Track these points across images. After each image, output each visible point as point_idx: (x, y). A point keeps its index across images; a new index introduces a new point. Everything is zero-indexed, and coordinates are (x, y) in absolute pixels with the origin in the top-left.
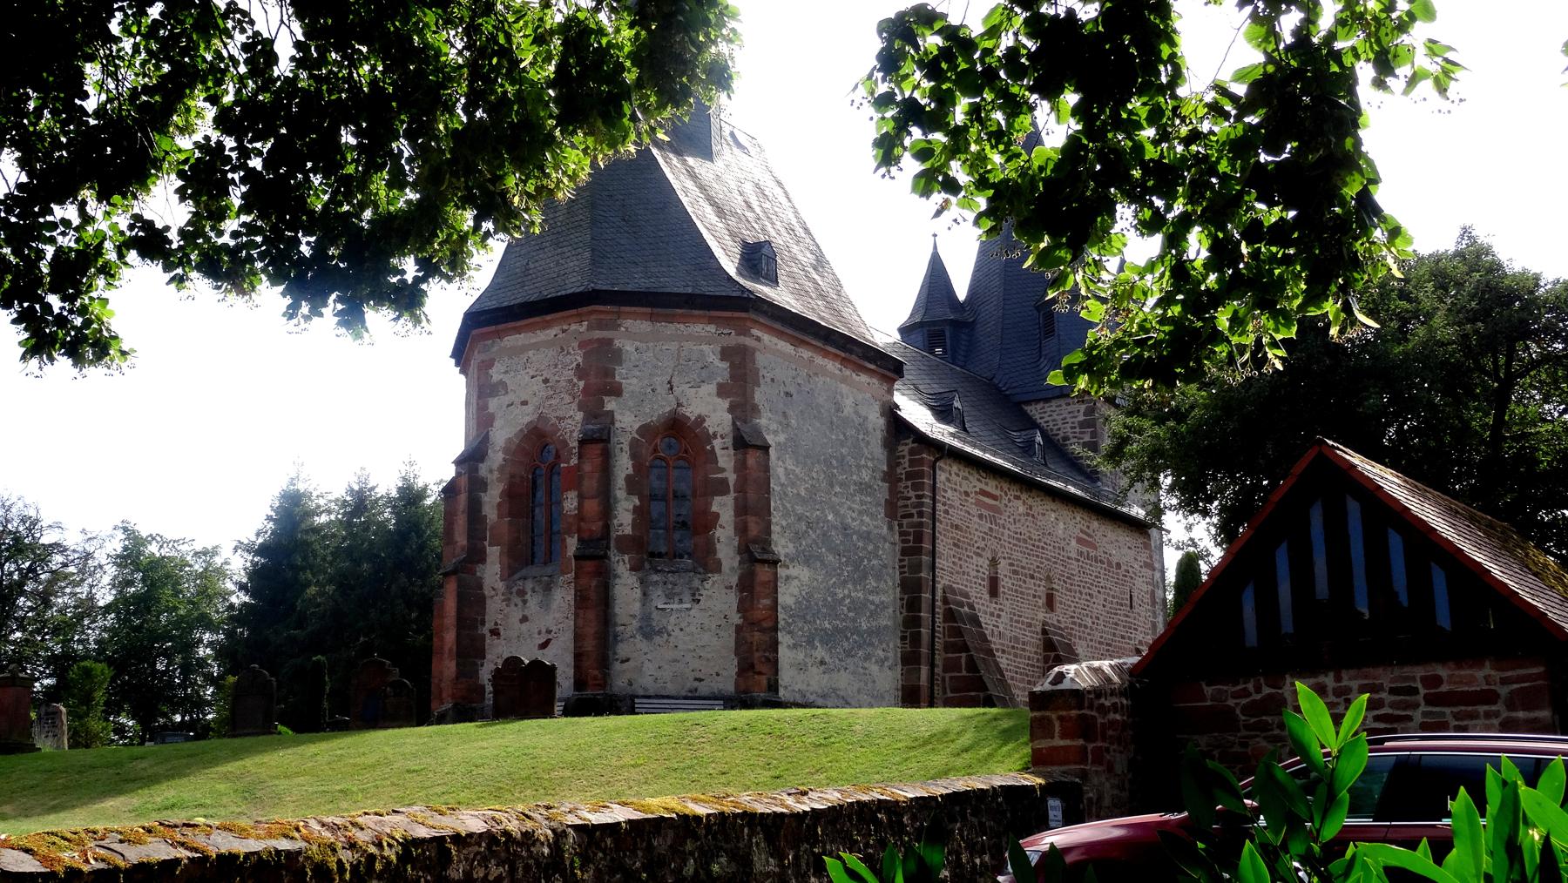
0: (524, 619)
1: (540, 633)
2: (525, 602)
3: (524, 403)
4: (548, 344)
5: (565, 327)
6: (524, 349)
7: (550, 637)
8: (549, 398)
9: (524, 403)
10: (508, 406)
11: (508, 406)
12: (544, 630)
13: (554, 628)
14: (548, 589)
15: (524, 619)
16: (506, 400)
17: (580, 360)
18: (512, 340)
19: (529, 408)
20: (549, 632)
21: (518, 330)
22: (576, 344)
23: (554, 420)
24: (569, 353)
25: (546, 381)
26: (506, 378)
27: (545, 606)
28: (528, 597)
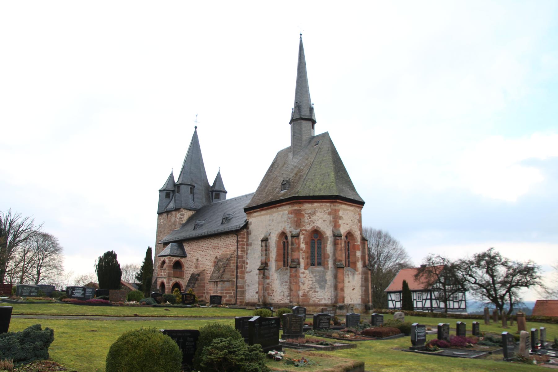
0: (349, 282)
1: (352, 286)
2: (349, 277)
3: (347, 224)
4: (352, 211)
6: (346, 210)
7: (355, 287)
8: (353, 225)
9: (347, 224)
13: (355, 285)
14: (354, 275)
15: (349, 282)
16: (344, 222)
18: (343, 206)
19: (348, 226)
21: (346, 204)
22: (357, 214)
23: (354, 231)
25: (352, 220)
26: (343, 216)
27: (353, 279)
28: (350, 276)
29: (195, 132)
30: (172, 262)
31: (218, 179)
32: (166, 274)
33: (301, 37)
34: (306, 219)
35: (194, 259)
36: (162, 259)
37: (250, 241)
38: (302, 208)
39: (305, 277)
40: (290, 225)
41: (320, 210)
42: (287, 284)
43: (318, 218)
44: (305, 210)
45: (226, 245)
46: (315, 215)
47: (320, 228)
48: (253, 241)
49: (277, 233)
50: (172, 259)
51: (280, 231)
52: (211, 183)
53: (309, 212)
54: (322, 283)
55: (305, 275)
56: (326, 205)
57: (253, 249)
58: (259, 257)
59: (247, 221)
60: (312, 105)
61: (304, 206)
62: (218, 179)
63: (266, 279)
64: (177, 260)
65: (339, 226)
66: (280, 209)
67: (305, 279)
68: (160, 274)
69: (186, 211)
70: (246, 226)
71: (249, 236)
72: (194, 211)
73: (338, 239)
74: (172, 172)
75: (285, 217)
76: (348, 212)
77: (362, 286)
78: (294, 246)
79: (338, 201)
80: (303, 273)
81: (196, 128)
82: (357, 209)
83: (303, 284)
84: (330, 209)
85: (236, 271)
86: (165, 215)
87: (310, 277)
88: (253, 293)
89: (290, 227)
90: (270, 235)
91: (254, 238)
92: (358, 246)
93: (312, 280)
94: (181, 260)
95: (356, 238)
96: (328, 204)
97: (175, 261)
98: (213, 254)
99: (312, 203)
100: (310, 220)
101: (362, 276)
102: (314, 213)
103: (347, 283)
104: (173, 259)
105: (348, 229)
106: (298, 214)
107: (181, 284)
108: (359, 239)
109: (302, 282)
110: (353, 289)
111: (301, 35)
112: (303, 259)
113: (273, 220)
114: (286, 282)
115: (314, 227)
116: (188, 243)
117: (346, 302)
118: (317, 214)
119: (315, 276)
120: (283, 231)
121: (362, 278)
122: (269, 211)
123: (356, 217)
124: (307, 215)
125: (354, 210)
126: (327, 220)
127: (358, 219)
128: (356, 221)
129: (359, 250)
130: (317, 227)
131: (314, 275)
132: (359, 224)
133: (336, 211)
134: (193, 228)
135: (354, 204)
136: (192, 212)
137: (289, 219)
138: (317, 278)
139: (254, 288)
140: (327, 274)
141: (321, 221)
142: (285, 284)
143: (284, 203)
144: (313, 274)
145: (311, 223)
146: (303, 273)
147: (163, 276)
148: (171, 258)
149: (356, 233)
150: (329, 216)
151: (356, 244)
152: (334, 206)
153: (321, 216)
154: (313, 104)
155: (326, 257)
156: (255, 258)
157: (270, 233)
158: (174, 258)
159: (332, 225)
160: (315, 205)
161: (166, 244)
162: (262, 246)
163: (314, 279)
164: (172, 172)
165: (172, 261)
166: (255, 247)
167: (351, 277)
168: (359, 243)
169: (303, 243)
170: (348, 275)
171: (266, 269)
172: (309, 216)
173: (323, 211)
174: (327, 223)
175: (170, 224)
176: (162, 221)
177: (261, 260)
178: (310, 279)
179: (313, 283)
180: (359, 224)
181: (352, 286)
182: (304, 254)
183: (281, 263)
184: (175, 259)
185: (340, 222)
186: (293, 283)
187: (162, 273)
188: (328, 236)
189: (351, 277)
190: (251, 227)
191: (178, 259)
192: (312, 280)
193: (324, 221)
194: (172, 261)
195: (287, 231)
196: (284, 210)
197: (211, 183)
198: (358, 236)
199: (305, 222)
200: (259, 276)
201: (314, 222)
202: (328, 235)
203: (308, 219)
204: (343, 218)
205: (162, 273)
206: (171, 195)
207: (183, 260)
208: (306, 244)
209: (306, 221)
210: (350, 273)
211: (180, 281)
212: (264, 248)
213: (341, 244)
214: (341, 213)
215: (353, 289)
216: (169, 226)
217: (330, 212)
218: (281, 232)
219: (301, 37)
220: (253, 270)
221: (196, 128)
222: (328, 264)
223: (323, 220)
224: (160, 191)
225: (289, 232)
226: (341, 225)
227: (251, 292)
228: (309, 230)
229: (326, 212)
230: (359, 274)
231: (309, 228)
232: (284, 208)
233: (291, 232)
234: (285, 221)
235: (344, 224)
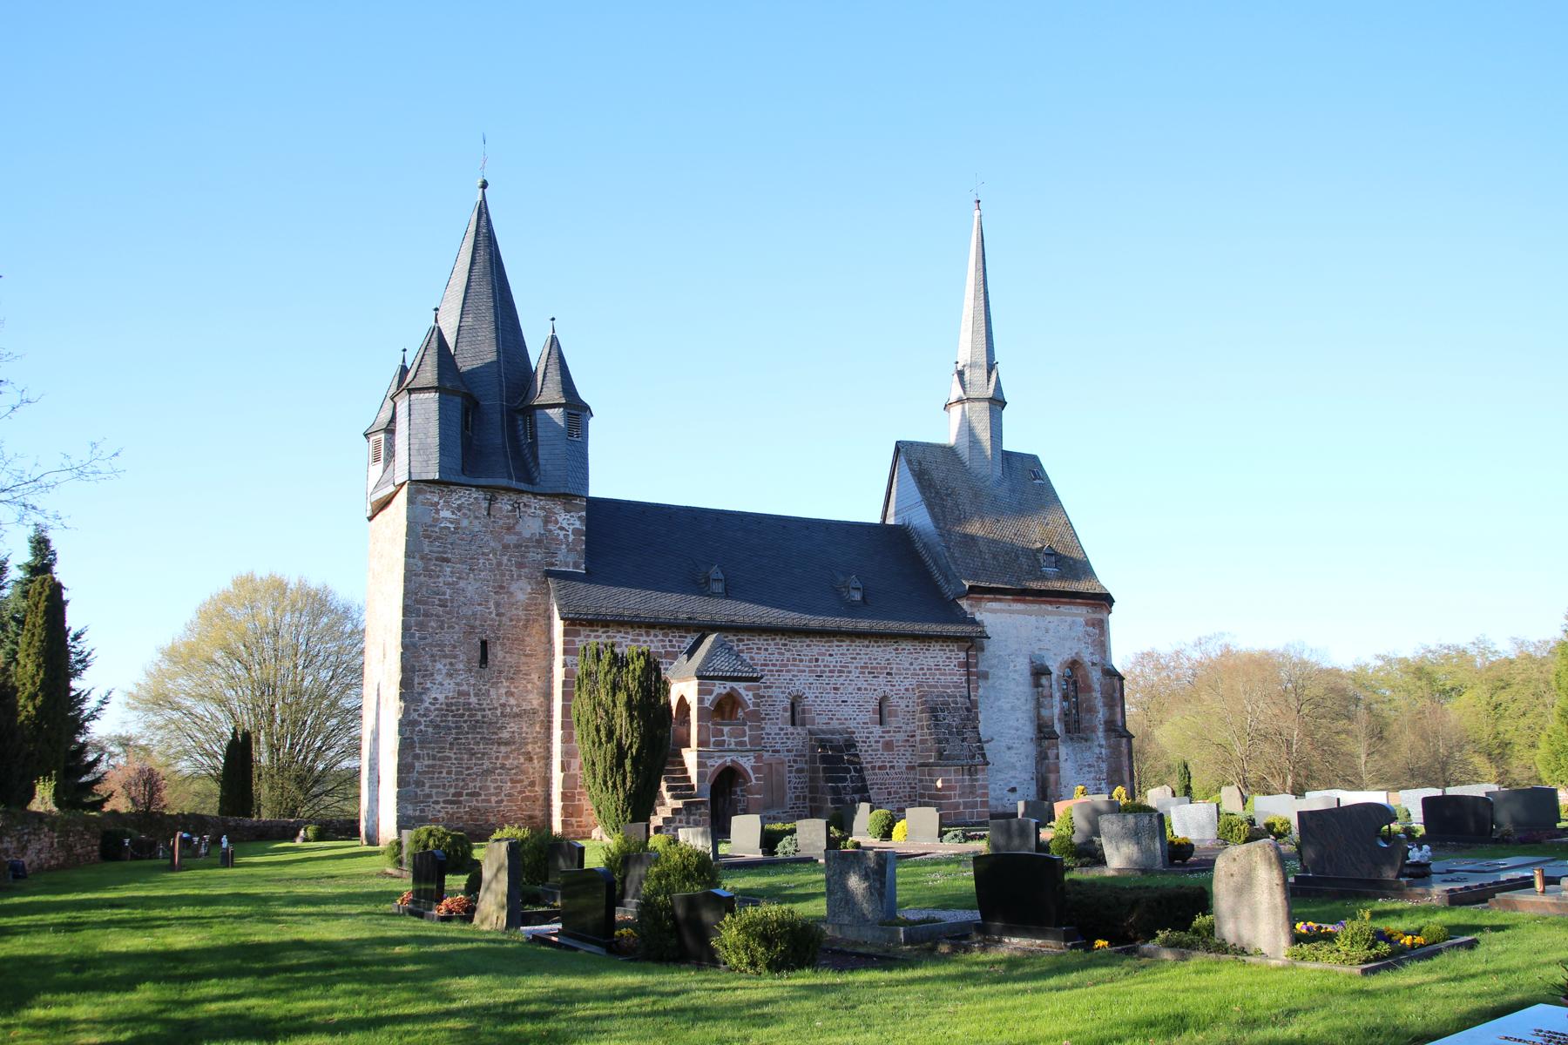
37: (982, 667)
45: (923, 669)
48: (991, 668)
49: (1060, 659)
51: (1067, 656)
57: (993, 687)
66: (1063, 609)
74: (436, 321)
88: (998, 792)
89: (1092, 654)
91: (995, 661)
114: (1090, 766)
122: (1035, 607)
137: (1089, 635)
139: (1002, 780)
142: (1087, 769)
143: (1078, 601)
147: (732, 747)
156: (1000, 710)
164: (436, 321)
166: (1001, 684)
184: (720, 689)
196: (1076, 615)
220: (995, 737)
221: (484, 185)
227: (995, 790)
232: (1074, 609)
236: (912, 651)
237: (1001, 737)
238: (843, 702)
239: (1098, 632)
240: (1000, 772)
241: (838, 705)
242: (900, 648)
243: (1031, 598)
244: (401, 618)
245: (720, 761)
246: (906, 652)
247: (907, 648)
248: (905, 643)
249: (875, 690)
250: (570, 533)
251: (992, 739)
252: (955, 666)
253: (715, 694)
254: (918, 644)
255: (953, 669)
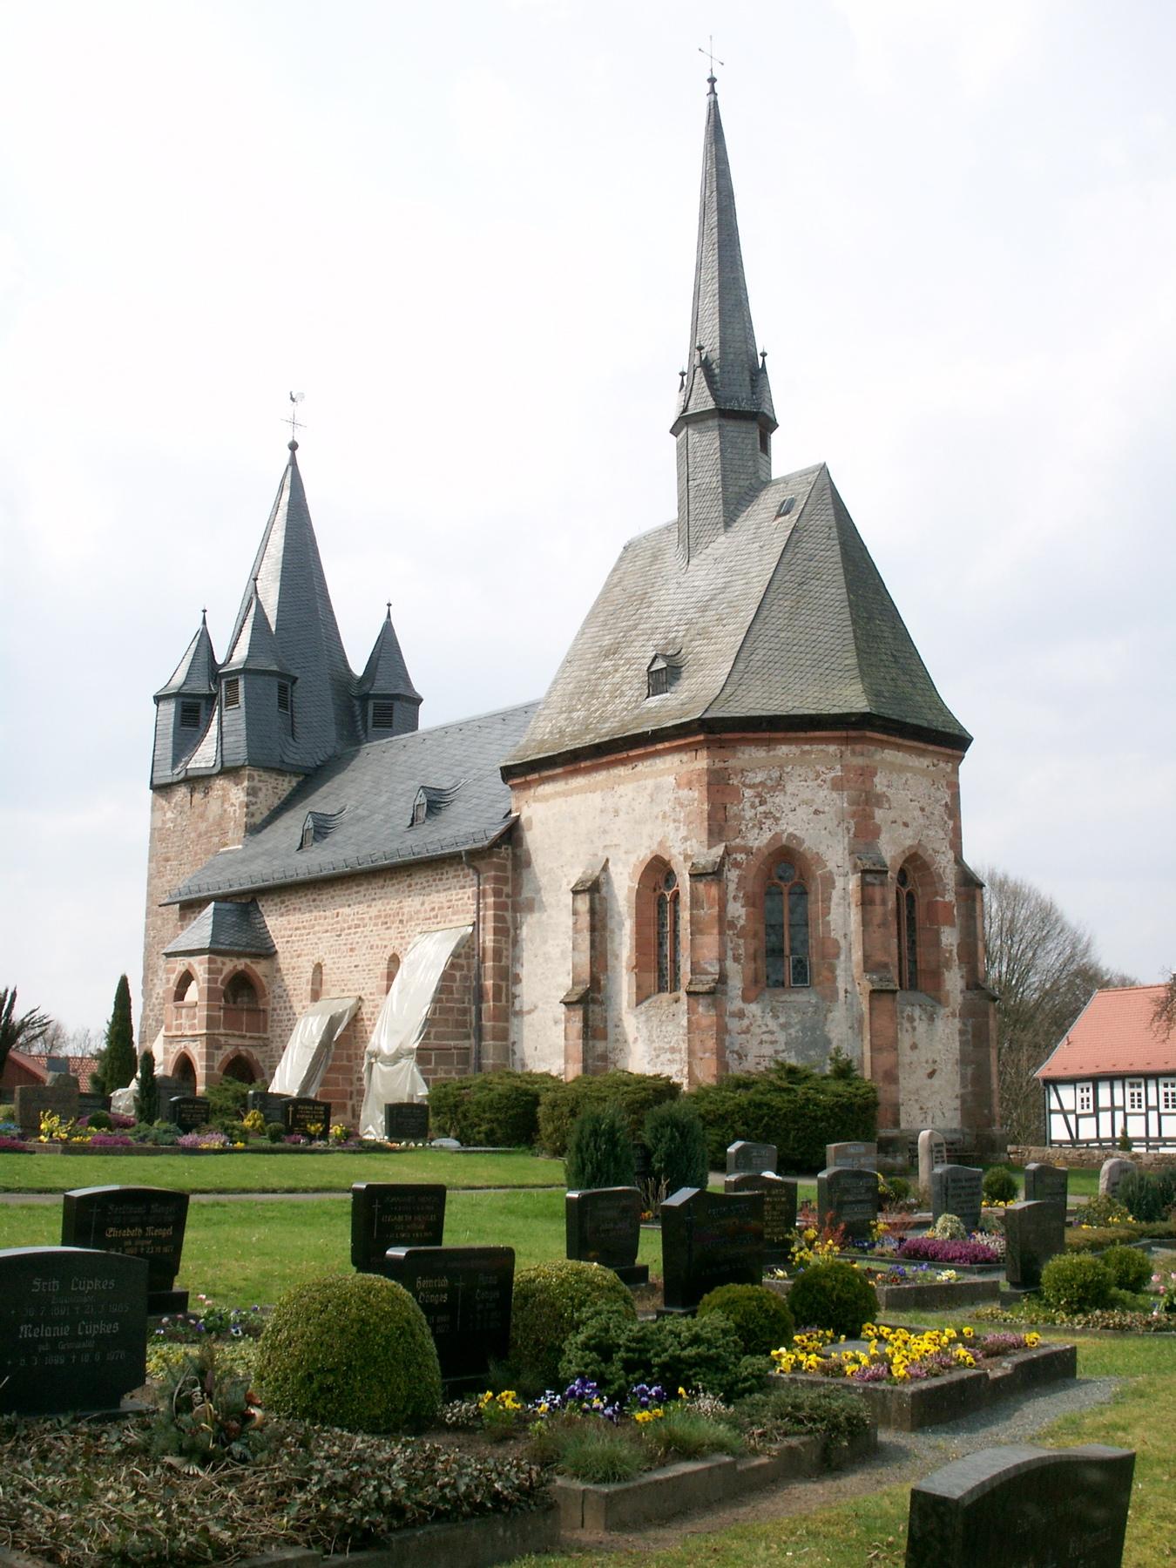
1: (927, 1062)
2: (914, 1029)
3: (906, 825)
4: (924, 772)
5: (936, 762)
6: (902, 769)
8: (927, 827)
9: (906, 825)
10: (893, 822)
11: (893, 822)
12: (930, 1061)
15: (914, 1047)
16: (892, 815)
17: (948, 800)
18: (889, 755)
19: (910, 832)
20: (934, 1062)
21: (898, 747)
22: (944, 783)
23: (930, 852)
24: (939, 789)
25: (922, 809)
26: (890, 792)
28: (916, 1024)
29: (293, 462)
30: (221, 978)
31: (387, 647)
32: (196, 1021)
33: (713, 91)
34: (746, 808)
35: (306, 964)
36: (180, 965)
38: (732, 763)
39: (747, 1031)
40: (683, 832)
41: (801, 771)
42: (677, 1056)
43: (795, 803)
44: (742, 770)
45: (433, 909)
46: (783, 790)
47: (801, 841)
49: (633, 859)
50: (219, 965)
51: (644, 854)
52: (358, 666)
53: (758, 780)
54: (812, 1053)
55: (746, 1022)
56: (822, 751)
58: (563, 952)
59: (513, 815)
60: (760, 359)
61: (740, 755)
62: (387, 646)
63: (594, 1037)
64: (240, 967)
65: (876, 832)
66: (642, 767)
67: (749, 1036)
68: (174, 1023)
69: (265, 776)
70: (512, 834)
71: (525, 873)
72: (295, 774)
73: (873, 885)
74: (204, 622)
75: (666, 802)
76: (909, 775)
77: (964, 1061)
78: (702, 912)
79: (869, 734)
80: (741, 1015)
81: (293, 447)
82: (942, 765)
83: (740, 1058)
84: (839, 767)
85: (474, 1008)
86: (181, 793)
87: (764, 1029)
89: (685, 839)
90: (605, 868)
92: (948, 906)
93: (772, 1043)
94: (253, 966)
95: (939, 876)
96: (832, 748)
97: (231, 972)
98: (379, 943)
99: (770, 743)
100: (761, 809)
101: (965, 1024)
102: (779, 786)
103: (908, 1051)
104: (224, 964)
105: (908, 842)
106: (719, 787)
107: (257, 1062)
108: (950, 877)
109: (736, 1048)
110: (931, 1075)
111: (712, 80)
112: (736, 959)
113: (616, 813)
114: (673, 1050)
115: (777, 836)
116: (277, 900)
117: (903, 1125)
118: (790, 788)
119: (784, 1027)
120: (659, 853)
121: (962, 1033)
122: (601, 776)
123: (939, 794)
124: (748, 793)
125: (932, 768)
126: (827, 809)
127: (946, 804)
128: (939, 811)
129: (952, 925)
130: (792, 836)
131: (782, 1020)
132: (951, 823)
133: (867, 773)
134: (298, 845)
135: (931, 748)
136: (287, 779)
137: (682, 805)
138: (792, 1031)
140: (830, 1016)
141: (803, 813)
142: (669, 1056)
143: (660, 746)
144: (776, 1017)
145: (768, 822)
146: (741, 1015)
148: (215, 962)
149: (939, 858)
150: (835, 795)
151: (939, 898)
152: (853, 753)
153: (807, 795)
154: (764, 355)
155: (831, 952)
157: (607, 860)
158: (227, 960)
159: (848, 829)
160: (783, 750)
161: (190, 907)
162: (575, 913)
163: (781, 1037)
164: (204, 622)
165: (220, 971)
167: (921, 1027)
168: (950, 897)
169: (735, 898)
170: (911, 1019)
171: (595, 1001)
172: (759, 795)
173: (812, 775)
174: (829, 819)
175: (203, 826)
176: (169, 815)
177: (574, 967)
178: (765, 1037)
179: (777, 1052)
180: (951, 823)
181: (927, 1062)
182: (741, 941)
183: (652, 978)
184: (229, 965)
185: (879, 814)
186: (700, 1055)
187: (183, 1021)
188: (835, 870)
189: (921, 1027)
190: (534, 839)
191: (241, 964)
192: (772, 1043)
193: (816, 812)
194: (220, 971)
195: (675, 851)
196: (662, 773)
197: (358, 666)
198: (948, 871)
199: (743, 818)
200: (566, 1028)
201: (777, 819)
202: (831, 866)
203: (753, 806)
204: (888, 800)
205: (183, 1021)
206: (203, 714)
207: (260, 968)
208: (750, 901)
209: (749, 814)
210: (917, 1012)
211: (251, 1049)
212: (585, 920)
213: (884, 902)
214: (880, 783)
215: (931, 1075)
216: (200, 836)
217: (841, 778)
218: (649, 857)
219: (713, 91)
220: (540, 1005)
221: (293, 447)
222: (834, 979)
223: (812, 809)
224: (158, 699)
225: (681, 858)
226: (884, 829)
228: (759, 849)
229: (823, 777)
230: (953, 1014)
231: (759, 840)
232: (662, 764)
233: (687, 857)
234: (664, 817)
235: (895, 822)
236: (425, 884)
237: (547, 1003)
238: (356, 966)
239: (696, 794)
240: (544, 1060)
241: (351, 972)
242: (413, 882)
243: (588, 763)
244: (144, 920)
245: (178, 1047)
246: (418, 887)
247: (419, 881)
248: (418, 876)
249: (386, 947)
250: (237, 808)
251: (536, 1007)
252: (469, 898)
253: (224, 973)
254: (430, 873)
255: (467, 904)
